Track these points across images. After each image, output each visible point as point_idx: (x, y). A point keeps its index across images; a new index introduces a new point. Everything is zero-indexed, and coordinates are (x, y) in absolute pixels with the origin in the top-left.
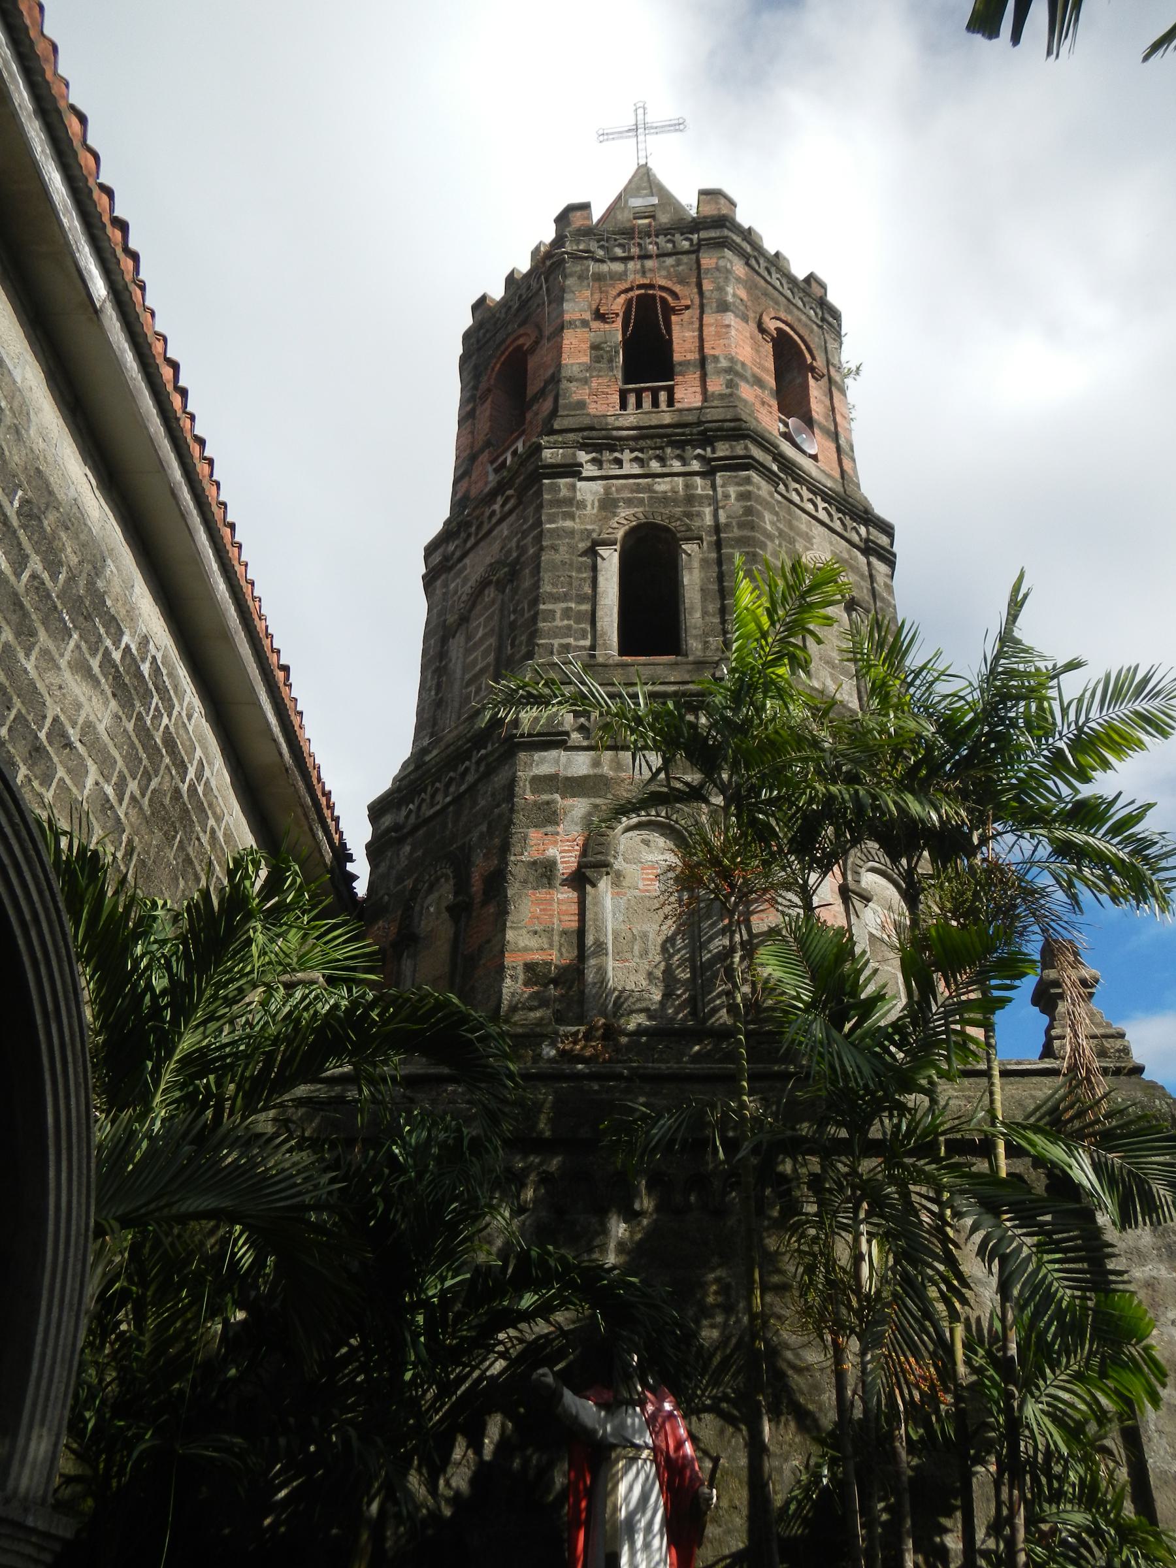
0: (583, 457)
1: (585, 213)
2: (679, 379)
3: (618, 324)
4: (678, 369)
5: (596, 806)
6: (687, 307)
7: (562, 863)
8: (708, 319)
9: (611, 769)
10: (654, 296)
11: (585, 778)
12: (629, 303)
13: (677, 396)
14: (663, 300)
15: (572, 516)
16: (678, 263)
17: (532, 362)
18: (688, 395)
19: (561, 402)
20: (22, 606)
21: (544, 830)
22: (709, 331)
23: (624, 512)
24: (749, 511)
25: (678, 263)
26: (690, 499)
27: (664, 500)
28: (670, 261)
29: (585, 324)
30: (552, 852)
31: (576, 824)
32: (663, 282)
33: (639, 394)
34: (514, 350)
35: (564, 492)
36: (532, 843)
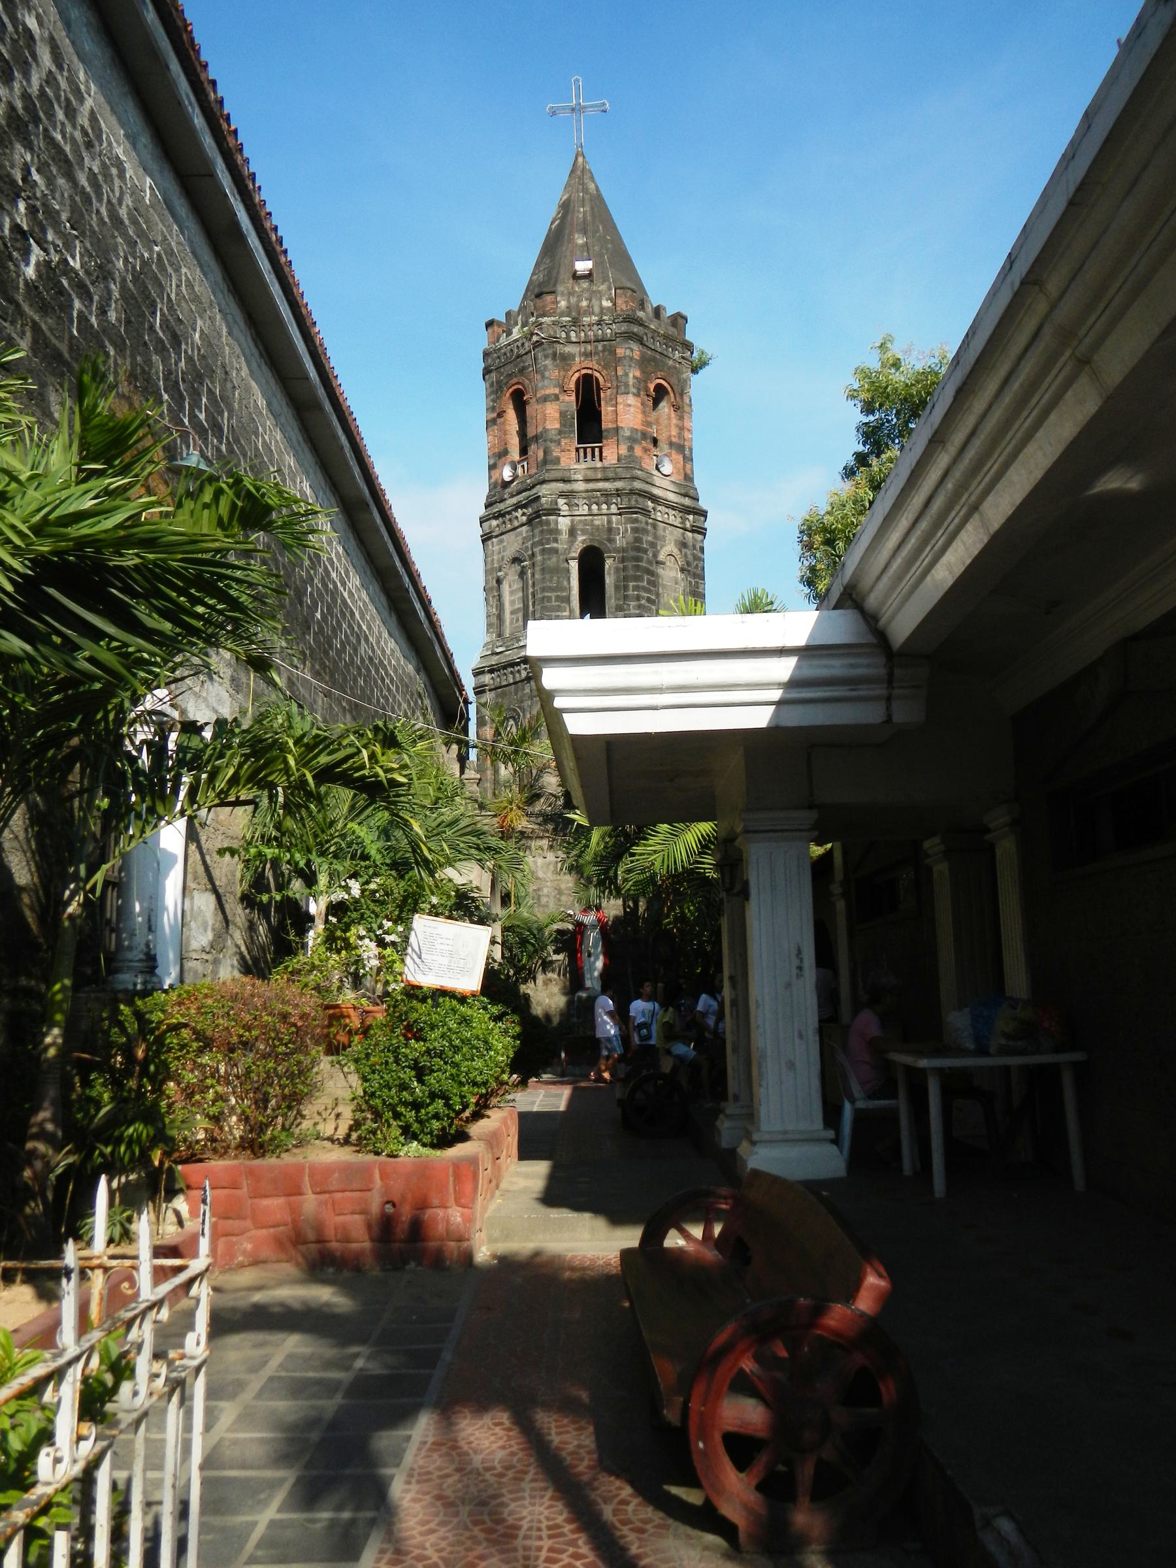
0: (561, 501)
3: (573, 398)
4: (604, 434)
8: (620, 399)
10: (591, 376)
12: (578, 379)
14: (597, 379)
15: (556, 540)
18: (611, 453)
19: (549, 458)
22: (620, 407)
23: (580, 538)
24: (638, 540)
26: (610, 530)
27: (597, 528)
29: (557, 398)
32: (596, 367)
33: (585, 449)
35: (552, 526)
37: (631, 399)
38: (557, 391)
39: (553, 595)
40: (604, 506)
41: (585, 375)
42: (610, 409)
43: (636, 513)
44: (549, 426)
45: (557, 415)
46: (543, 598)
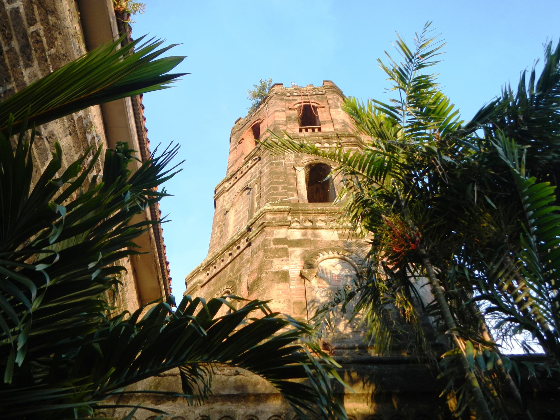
1: (281, 86)
2: (322, 125)
5: (306, 251)
6: (323, 107)
7: (291, 273)
9: (312, 237)
10: (310, 106)
11: (299, 240)
13: (323, 129)
16: (318, 97)
17: (261, 126)
20: (27, 40)
21: (281, 259)
25: (318, 97)
28: (315, 97)
30: (285, 268)
31: (297, 258)
32: (313, 101)
34: (254, 126)
36: (275, 264)
37: (340, 110)
38: (284, 109)
39: (280, 186)
40: (327, 145)
41: (305, 106)
42: (324, 114)
43: (356, 145)
44: (276, 119)
45: (285, 116)
46: (269, 190)
